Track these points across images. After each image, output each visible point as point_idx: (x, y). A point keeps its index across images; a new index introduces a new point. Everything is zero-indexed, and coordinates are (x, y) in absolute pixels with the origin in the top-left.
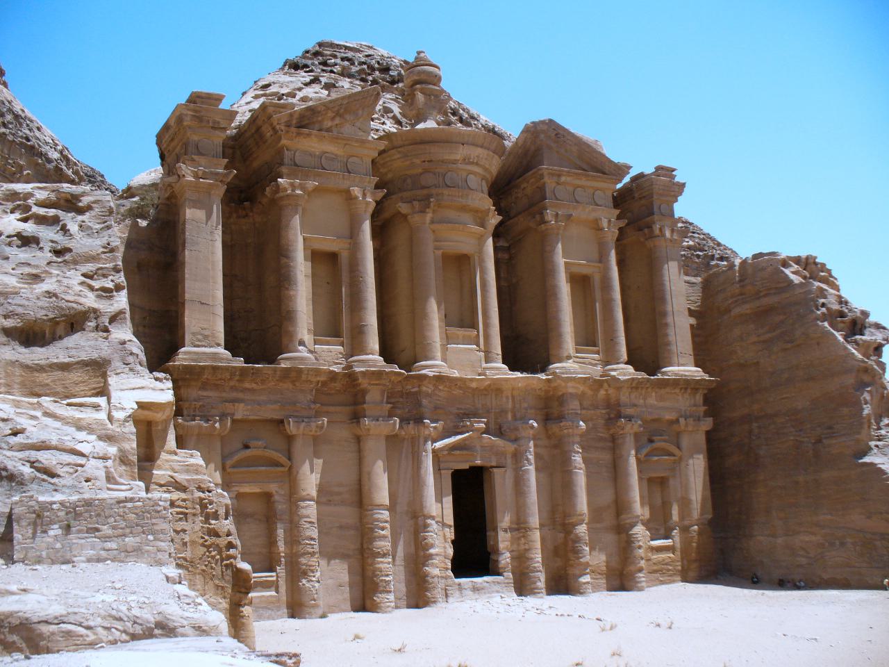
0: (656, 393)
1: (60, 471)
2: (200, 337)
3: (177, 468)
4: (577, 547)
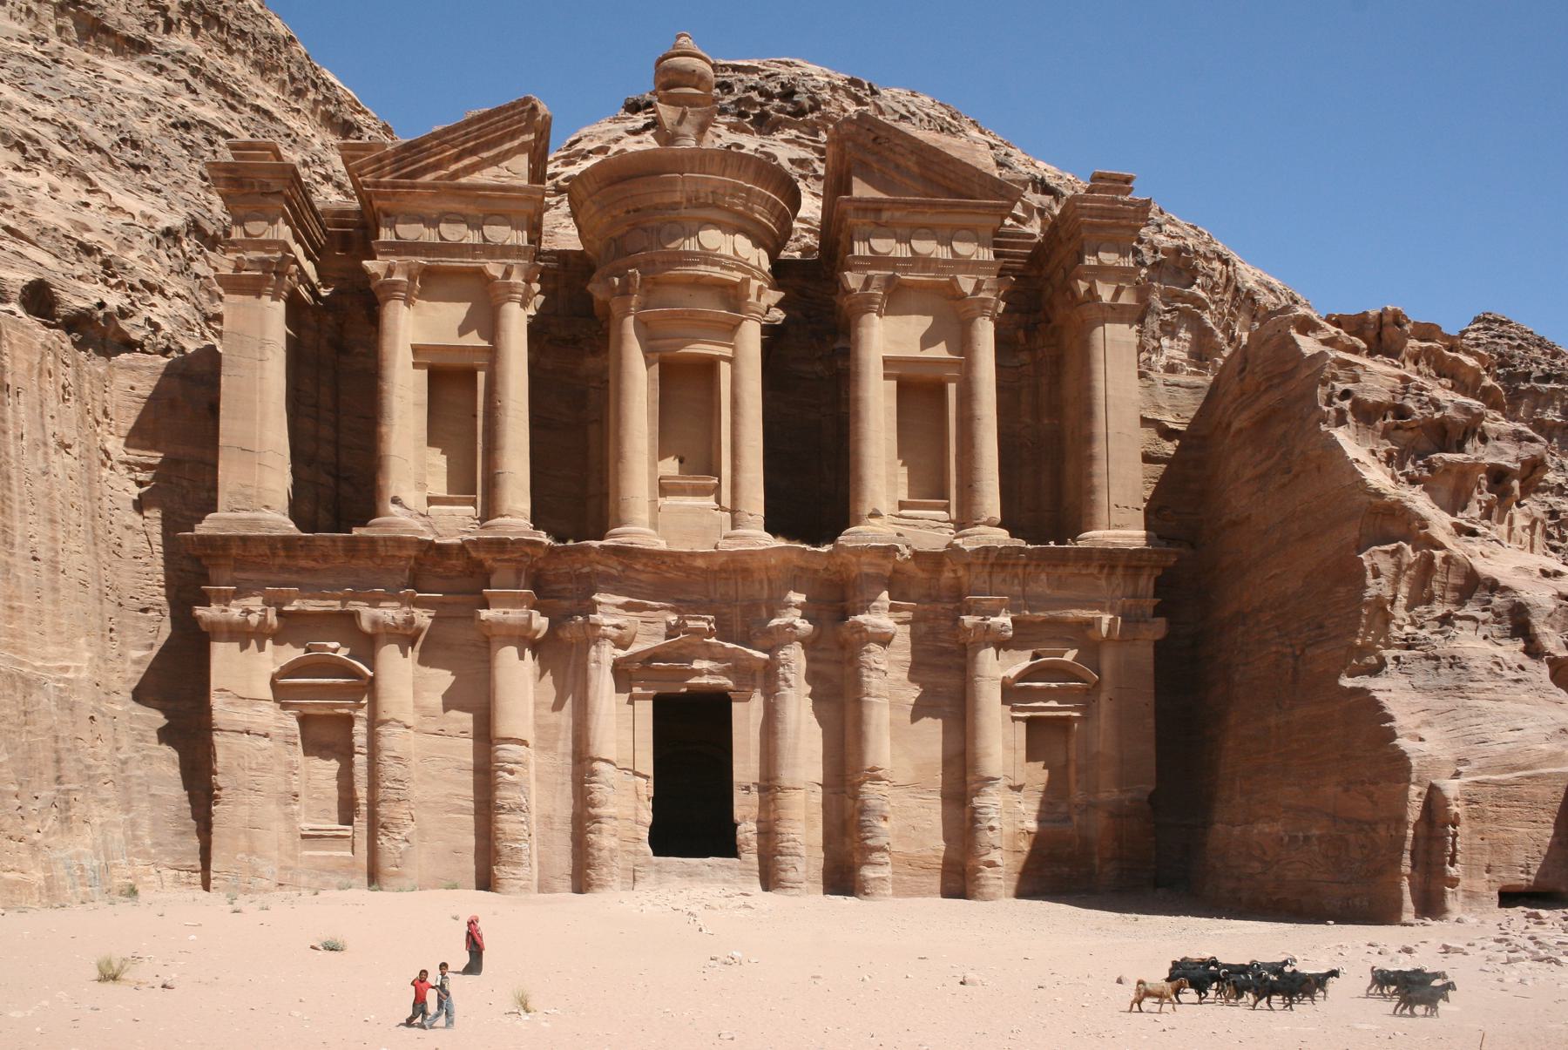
0: (1048, 574)
2: (239, 497)
4: (864, 821)
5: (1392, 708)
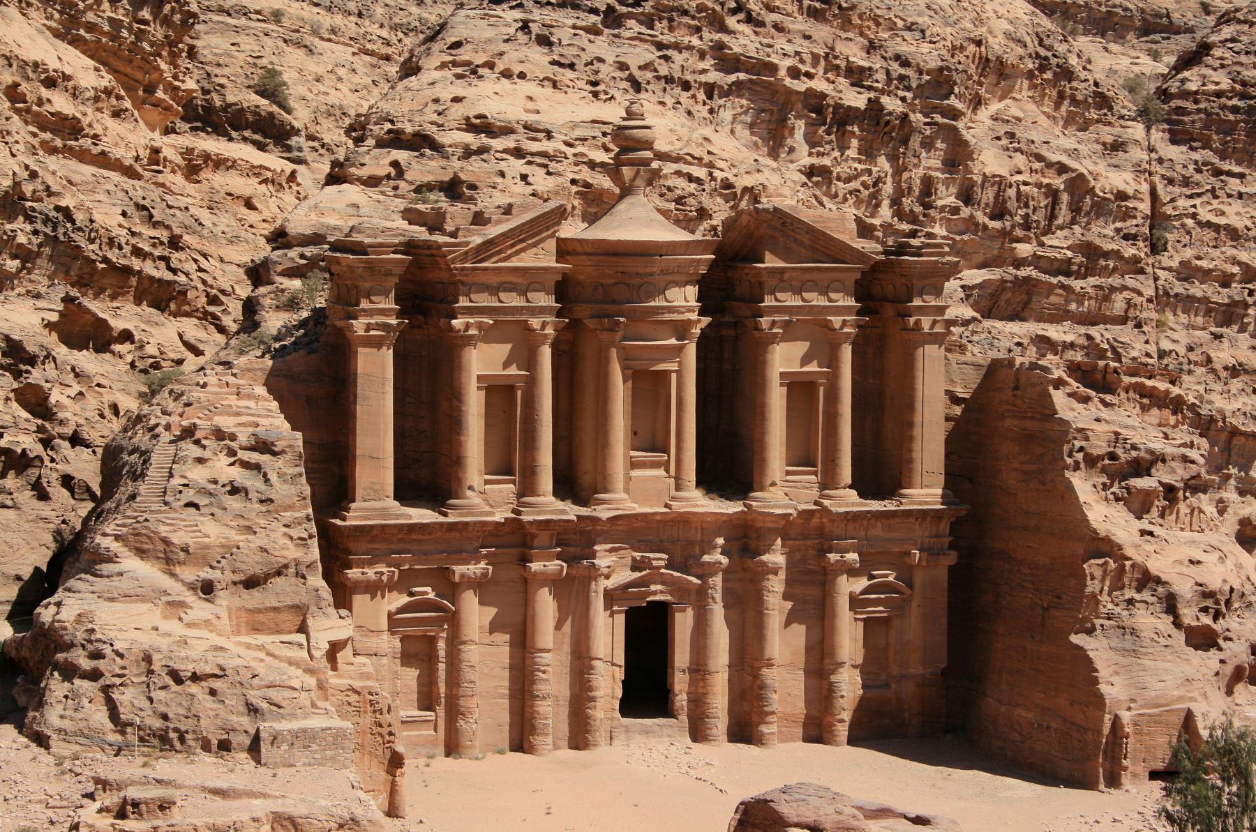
1: (283, 704)
3: (353, 674)
5: (1098, 664)
